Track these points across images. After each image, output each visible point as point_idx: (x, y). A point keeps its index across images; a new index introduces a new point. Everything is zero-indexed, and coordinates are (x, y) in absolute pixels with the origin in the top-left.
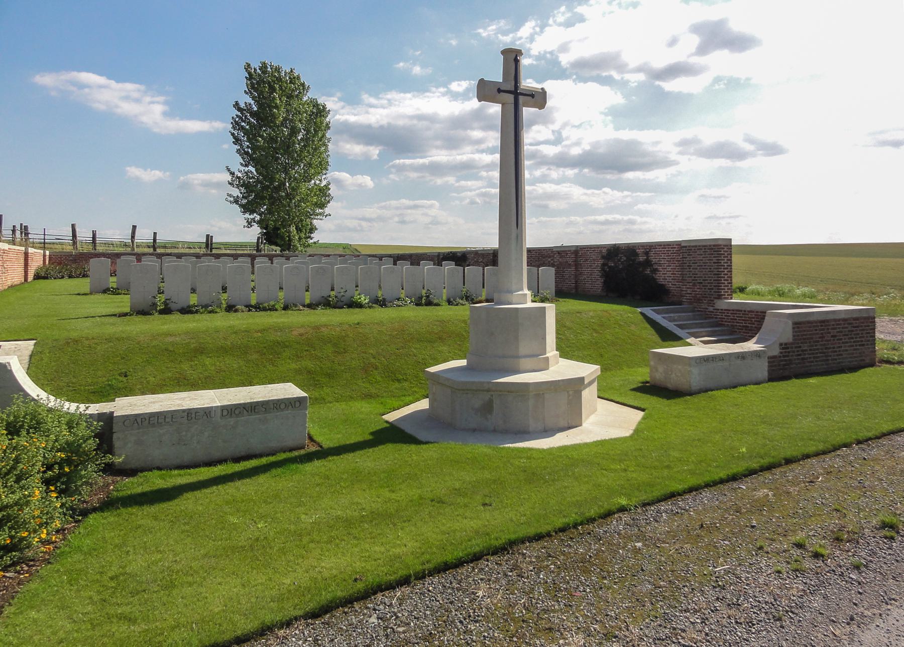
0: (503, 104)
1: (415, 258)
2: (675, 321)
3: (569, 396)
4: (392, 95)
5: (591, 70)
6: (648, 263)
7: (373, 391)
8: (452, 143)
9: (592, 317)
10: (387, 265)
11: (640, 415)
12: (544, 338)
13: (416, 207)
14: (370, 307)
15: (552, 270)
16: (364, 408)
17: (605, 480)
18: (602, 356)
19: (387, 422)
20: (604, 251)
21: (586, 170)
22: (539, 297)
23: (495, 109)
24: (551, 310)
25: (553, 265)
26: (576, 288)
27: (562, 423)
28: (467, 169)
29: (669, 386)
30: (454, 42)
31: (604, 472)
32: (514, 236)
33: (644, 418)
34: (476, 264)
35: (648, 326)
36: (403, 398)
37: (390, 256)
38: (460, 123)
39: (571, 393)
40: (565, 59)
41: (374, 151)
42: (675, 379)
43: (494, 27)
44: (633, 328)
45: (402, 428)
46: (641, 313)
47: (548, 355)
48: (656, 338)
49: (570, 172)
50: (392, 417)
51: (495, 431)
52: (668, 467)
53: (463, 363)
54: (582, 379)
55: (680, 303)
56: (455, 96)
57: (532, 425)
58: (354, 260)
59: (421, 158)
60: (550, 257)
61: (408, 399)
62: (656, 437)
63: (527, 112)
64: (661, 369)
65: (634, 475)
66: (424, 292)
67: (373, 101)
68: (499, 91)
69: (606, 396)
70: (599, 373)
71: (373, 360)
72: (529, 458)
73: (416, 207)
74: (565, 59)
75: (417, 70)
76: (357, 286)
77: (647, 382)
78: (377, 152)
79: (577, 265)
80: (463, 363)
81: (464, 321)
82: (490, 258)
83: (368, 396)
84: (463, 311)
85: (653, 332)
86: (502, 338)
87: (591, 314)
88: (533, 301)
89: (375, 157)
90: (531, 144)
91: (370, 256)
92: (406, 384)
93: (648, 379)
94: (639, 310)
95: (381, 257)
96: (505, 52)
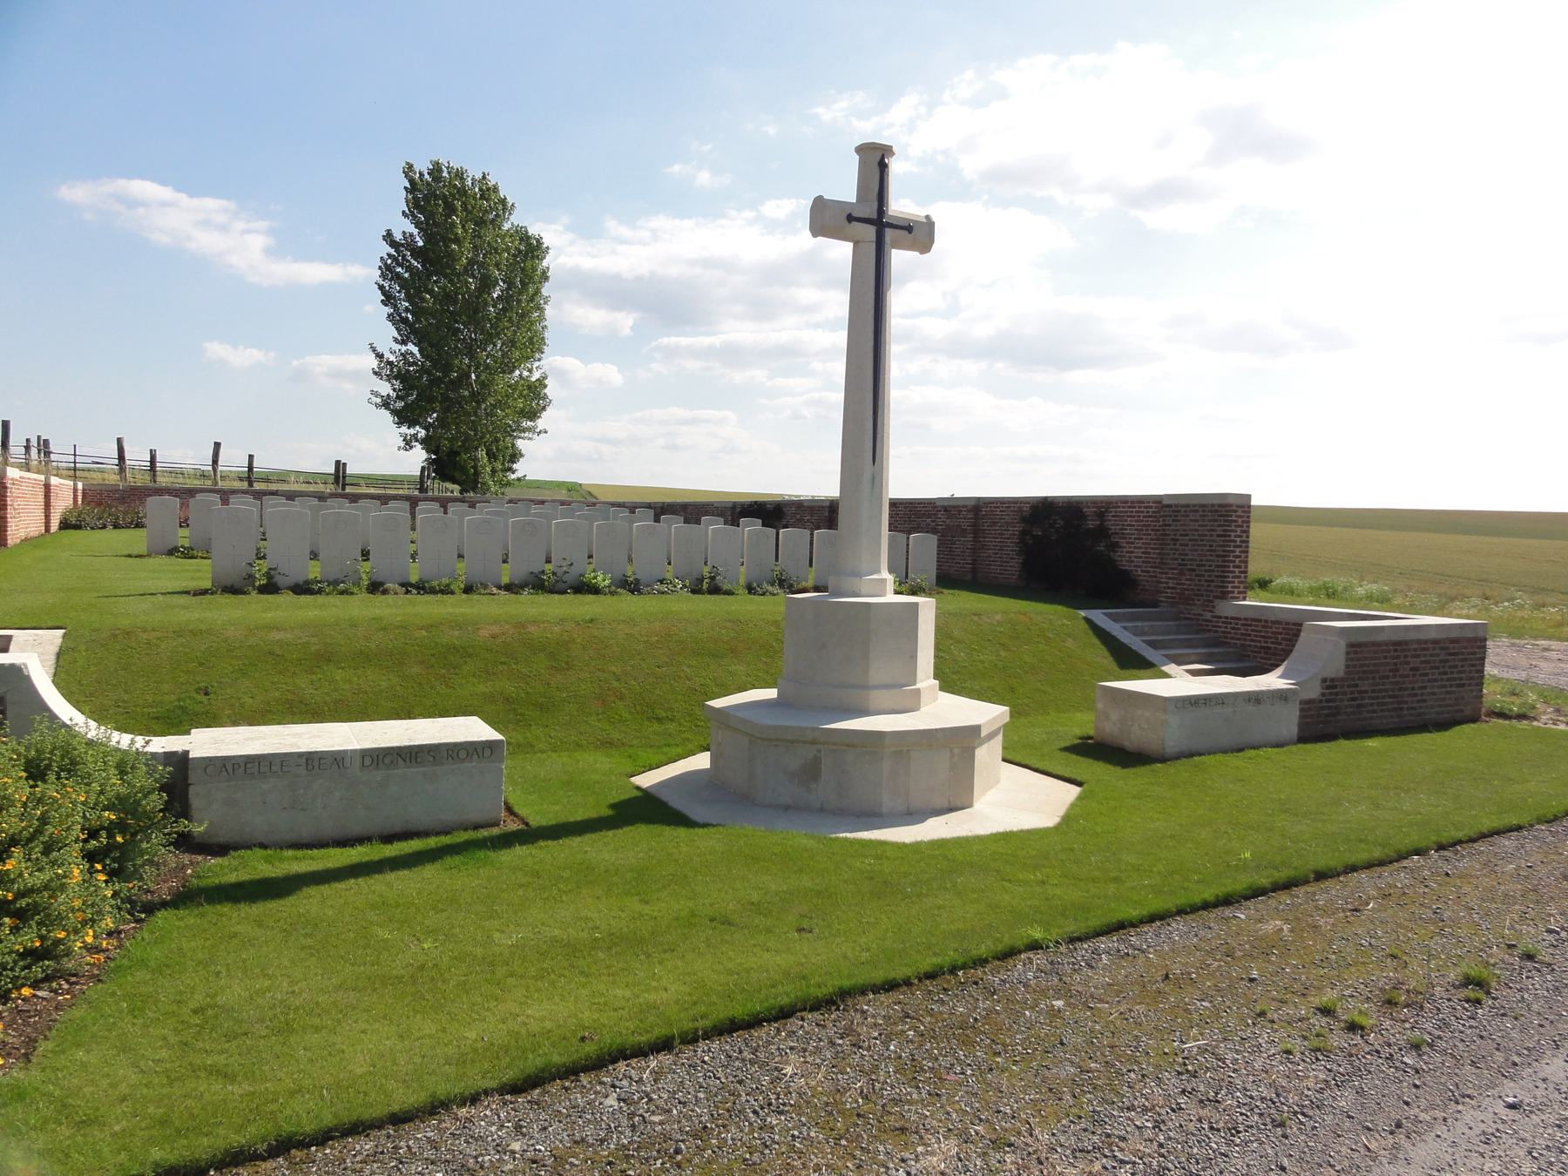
0: (856, 243)
1: (692, 511)
2: (1143, 634)
3: (953, 756)
4: (660, 222)
5: (1010, 185)
6: (1102, 532)
7: (616, 735)
8: (762, 310)
9: (999, 623)
10: (644, 522)
11: (1073, 791)
12: (913, 657)
13: (695, 421)
14: (613, 593)
15: (932, 541)
16: (598, 764)
17: (1007, 897)
18: (1013, 690)
19: (638, 788)
20: (1026, 508)
21: (1000, 365)
22: (907, 585)
23: (840, 252)
24: (927, 607)
25: (934, 531)
26: (974, 571)
27: (940, 801)
28: (786, 357)
29: (1127, 745)
30: (772, 130)
31: (1007, 884)
32: (867, 476)
33: (1080, 798)
34: (800, 524)
35: (1097, 642)
36: (666, 749)
37: (649, 506)
38: (778, 274)
39: (956, 751)
40: (970, 166)
41: (626, 322)
42: (1137, 735)
43: (844, 104)
44: (1070, 643)
45: (664, 798)
46: (1087, 620)
47: (918, 686)
48: (1108, 661)
49: (972, 368)
50: (646, 780)
51: (822, 810)
52: (1116, 880)
53: (771, 693)
54: (976, 729)
55: (1155, 604)
56: (771, 226)
57: (887, 802)
58: (586, 511)
59: (709, 334)
60: (929, 516)
61: (674, 751)
62: (1099, 829)
63: (900, 259)
64: (1115, 716)
65: (1058, 892)
66: (706, 571)
67: (625, 231)
68: (850, 218)
69: (1018, 759)
70: (1007, 719)
71: (615, 684)
72: (877, 857)
73: (695, 421)
74: (970, 166)
75: (704, 178)
76: (590, 557)
77: (1090, 738)
78: (630, 322)
79: (977, 531)
80: (771, 693)
81: (776, 623)
82: (823, 515)
83: (607, 744)
84: (774, 605)
85: (1106, 653)
86: (845, 653)
87: (998, 617)
88: (897, 593)
89: (627, 331)
90: (904, 316)
91: (613, 505)
92: (671, 726)
93: (1092, 733)
94: (1082, 613)
95: (632, 508)
96: (865, 150)
